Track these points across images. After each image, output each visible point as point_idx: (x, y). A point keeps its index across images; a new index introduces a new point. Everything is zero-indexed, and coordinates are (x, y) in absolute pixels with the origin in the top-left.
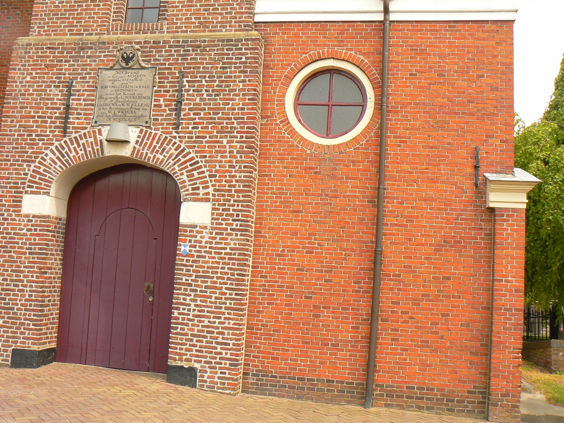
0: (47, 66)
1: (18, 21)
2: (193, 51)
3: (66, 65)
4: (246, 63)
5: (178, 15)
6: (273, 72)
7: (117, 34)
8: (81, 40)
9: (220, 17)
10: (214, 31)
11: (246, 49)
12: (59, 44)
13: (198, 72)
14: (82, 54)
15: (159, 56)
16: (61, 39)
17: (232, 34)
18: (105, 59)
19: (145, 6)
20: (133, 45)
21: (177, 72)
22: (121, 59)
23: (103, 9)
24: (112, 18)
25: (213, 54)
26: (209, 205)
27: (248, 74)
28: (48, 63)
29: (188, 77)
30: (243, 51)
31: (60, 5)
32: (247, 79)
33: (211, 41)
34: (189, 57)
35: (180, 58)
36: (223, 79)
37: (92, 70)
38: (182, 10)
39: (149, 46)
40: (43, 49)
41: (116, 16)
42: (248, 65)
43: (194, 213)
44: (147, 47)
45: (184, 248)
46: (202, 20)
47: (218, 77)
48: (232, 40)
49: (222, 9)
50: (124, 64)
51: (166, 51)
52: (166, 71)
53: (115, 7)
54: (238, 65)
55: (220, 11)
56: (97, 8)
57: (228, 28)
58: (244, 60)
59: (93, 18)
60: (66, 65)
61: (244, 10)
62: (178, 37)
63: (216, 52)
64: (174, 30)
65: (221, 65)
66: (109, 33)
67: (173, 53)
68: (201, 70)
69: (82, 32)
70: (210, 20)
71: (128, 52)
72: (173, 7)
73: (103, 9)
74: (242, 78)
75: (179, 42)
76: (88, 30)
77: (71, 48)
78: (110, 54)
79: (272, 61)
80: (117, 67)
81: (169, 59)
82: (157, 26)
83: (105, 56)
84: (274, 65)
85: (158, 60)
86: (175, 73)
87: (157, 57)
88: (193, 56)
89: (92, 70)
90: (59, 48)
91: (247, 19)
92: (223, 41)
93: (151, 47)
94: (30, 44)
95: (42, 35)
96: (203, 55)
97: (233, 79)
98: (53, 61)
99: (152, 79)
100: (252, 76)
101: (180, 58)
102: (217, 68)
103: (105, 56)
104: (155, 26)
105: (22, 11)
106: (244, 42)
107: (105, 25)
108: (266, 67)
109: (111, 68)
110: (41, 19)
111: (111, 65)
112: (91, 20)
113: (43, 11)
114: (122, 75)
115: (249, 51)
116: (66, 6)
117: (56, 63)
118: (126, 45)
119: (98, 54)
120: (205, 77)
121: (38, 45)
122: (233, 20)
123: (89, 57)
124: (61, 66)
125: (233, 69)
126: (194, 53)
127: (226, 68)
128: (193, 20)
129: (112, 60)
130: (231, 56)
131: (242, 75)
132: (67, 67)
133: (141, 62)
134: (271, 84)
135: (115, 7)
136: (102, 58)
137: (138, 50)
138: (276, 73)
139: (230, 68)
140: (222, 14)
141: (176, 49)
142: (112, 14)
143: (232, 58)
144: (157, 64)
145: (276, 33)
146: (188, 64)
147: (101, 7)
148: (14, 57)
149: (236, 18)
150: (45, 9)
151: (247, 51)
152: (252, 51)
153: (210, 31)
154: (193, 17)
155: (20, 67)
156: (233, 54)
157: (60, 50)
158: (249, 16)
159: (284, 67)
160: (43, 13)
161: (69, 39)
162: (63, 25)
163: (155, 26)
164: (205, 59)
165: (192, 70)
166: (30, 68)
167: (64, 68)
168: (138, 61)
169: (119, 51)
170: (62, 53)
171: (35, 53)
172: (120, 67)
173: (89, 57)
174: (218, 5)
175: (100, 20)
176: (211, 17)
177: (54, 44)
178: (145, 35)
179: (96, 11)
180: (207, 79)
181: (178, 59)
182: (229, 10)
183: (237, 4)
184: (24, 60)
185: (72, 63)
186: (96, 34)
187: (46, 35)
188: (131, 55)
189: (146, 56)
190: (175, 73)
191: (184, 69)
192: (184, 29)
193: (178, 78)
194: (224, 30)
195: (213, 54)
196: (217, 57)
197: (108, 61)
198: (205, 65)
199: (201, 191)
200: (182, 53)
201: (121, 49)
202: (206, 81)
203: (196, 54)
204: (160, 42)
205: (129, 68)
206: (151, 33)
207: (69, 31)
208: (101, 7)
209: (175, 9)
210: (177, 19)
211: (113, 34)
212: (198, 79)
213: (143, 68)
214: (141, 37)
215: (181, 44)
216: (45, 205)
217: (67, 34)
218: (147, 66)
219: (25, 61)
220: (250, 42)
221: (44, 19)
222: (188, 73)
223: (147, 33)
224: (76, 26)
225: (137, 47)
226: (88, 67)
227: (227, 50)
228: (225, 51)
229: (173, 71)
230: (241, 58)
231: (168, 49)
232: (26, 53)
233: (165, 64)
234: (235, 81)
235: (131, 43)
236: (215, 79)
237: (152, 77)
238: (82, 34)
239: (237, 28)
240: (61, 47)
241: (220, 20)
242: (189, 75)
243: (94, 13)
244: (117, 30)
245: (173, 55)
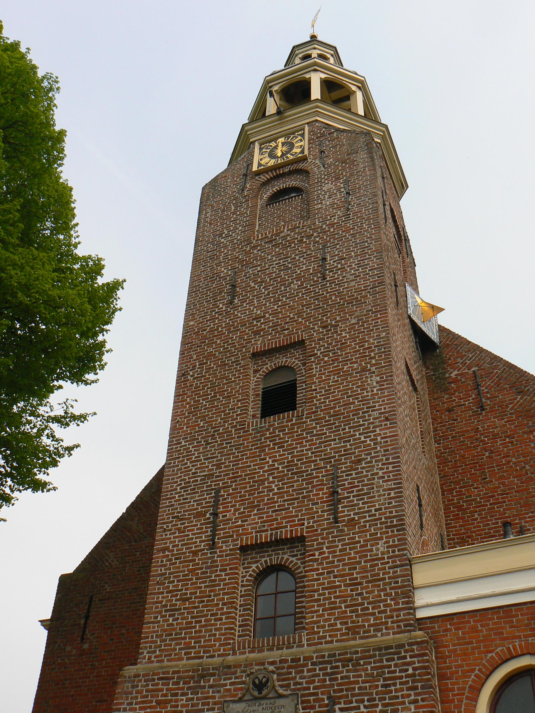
0: (158, 702)
1: (122, 642)
2: (343, 666)
3: (182, 700)
4: (413, 675)
5: (319, 622)
6: (452, 684)
7: (244, 653)
8: (200, 665)
9: (372, 619)
10: (367, 637)
11: (411, 657)
12: (174, 672)
13: (353, 695)
14: (202, 683)
15: (301, 678)
16: (176, 666)
17: (390, 638)
18: (232, 687)
19: (278, 614)
20: (267, 666)
21: (325, 697)
22: (251, 686)
23: (225, 624)
24: (237, 634)
25: (369, 668)
27: (420, 690)
28: (160, 698)
29: (340, 703)
30: (409, 659)
31: (175, 623)
32: (419, 698)
33: (365, 651)
34: (339, 676)
35: (327, 678)
36: (387, 701)
37: (215, 703)
38: (323, 615)
39: (286, 665)
40: (154, 680)
41: (242, 631)
42: (417, 678)
44: (283, 668)
46: (350, 625)
47: (380, 699)
48: (391, 647)
49: (373, 608)
50: (256, 693)
51: (308, 671)
52: (312, 698)
53: (241, 619)
54: (404, 679)
55: (371, 611)
56: (219, 623)
57: (384, 631)
58: (410, 671)
59: (215, 635)
60: (182, 700)
61: (401, 606)
62: (321, 650)
63: (373, 665)
64: (316, 641)
65: (382, 682)
66: (234, 654)
67: (317, 671)
68: (357, 691)
69: (202, 654)
70: (360, 623)
71: (260, 677)
72: (312, 612)
73: (225, 624)
74: (412, 697)
75: (323, 657)
76: (209, 651)
77: (188, 677)
78: (237, 680)
79: (449, 668)
80: (246, 698)
81: (314, 681)
82: (294, 639)
83: (231, 684)
84: (452, 674)
85: (300, 684)
86: (323, 700)
87: (298, 679)
88: (345, 674)
89: (215, 703)
90: (174, 678)
91: (407, 617)
92: (380, 649)
93: (289, 667)
94: (139, 676)
95: (153, 662)
96: (357, 671)
97: (400, 700)
98: (166, 695)
99: (294, 710)
100: (425, 693)
101: (327, 678)
102: (377, 686)
103: (231, 684)
104: (291, 639)
105: (128, 629)
106: (407, 647)
107: (229, 644)
108: (442, 677)
109: (240, 700)
110: (152, 642)
111: (240, 696)
112: (213, 638)
113: (154, 632)
114: (254, 708)
115: (416, 659)
116: (182, 623)
117: (169, 698)
118: (257, 667)
119: (222, 682)
120: (363, 701)
121: (148, 675)
122: (390, 620)
123: (211, 687)
124: (176, 701)
125: (398, 686)
126: (345, 669)
127: (389, 685)
128: (339, 626)
129: (241, 689)
130: (393, 668)
131: (412, 693)
132: (184, 702)
133: (278, 688)
134: (453, 701)
135: (241, 619)
136: (228, 687)
137: (273, 672)
138: (456, 684)
139: (395, 684)
140: (373, 614)
141: (321, 666)
142: (237, 628)
143: (395, 672)
144: (299, 689)
145: (447, 630)
146: (338, 685)
147: (224, 621)
148: (119, 693)
149: (393, 617)
150: (156, 629)
151: (413, 659)
152: (420, 659)
153: (362, 638)
154: (338, 622)
155: (125, 706)
156: (396, 665)
157: (175, 680)
158: (408, 613)
159: (466, 674)
160: (155, 635)
161: (185, 665)
162: (178, 647)
163: (291, 639)
164: (361, 676)
165: (345, 693)
166: (138, 706)
167: (180, 703)
168: (274, 687)
169: (248, 675)
170: (178, 683)
171: (145, 686)
172: (251, 698)
173: (211, 687)
174: (368, 604)
175: (223, 638)
176: (360, 619)
177: (168, 673)
178: (280, 652)
179: (218, 626)
180: (366, 703)
181: (325, 680)
182: (382, 608)
183: (391, 600)
184: (130, 696)
185: (190, 696)
186: (219, 656)
187: (158, 661)
188: (264, 680)
189: (284, 680)
190: (323, 700)
191: (334, 692)
192: (328, 639)
193: (327, 705)
194: (379, 634)
195: (369, 668)
196: (375, 672)
197: (235, 689)
198: (361, 685)
200: (329, 671)
201: (251, 673)
202: (365, 707)
203: (348, 671)
204: (300, 659)
205: (265, 698)
206: (287, 648)
207: (185, 654)
208: (224, 621)
209: (315, 615)
210: (318, 627)
211: (241, 653)
212: (354, 704)
213: (281, 696)
214: (275, 655)
215: (326, 659)
217: (183, 659)
218: (285, 693)
219: (132, 698)
220: (415, 647)
221: (156, 642)
222: (340, 697)
223: (282, 649)
224: (194, 647)
225: (271, 668)
226: (211, 701)
227: (387, 660)
228: (385, 663)
229: (320, 696)
230: (407, 670)
231: (310, 667)
232: (133, 687)
233: (309, 689)
234: (403, 703)
235: (263, 664)
236: (377, 702)
237: (294, 708)
238: (202, 657)
239: (396, 630)
240: (176, 676)
241: (372, 622)
242: (342, 701)
243: (216, 630)
244: (244, 648)
245: (319, 675)
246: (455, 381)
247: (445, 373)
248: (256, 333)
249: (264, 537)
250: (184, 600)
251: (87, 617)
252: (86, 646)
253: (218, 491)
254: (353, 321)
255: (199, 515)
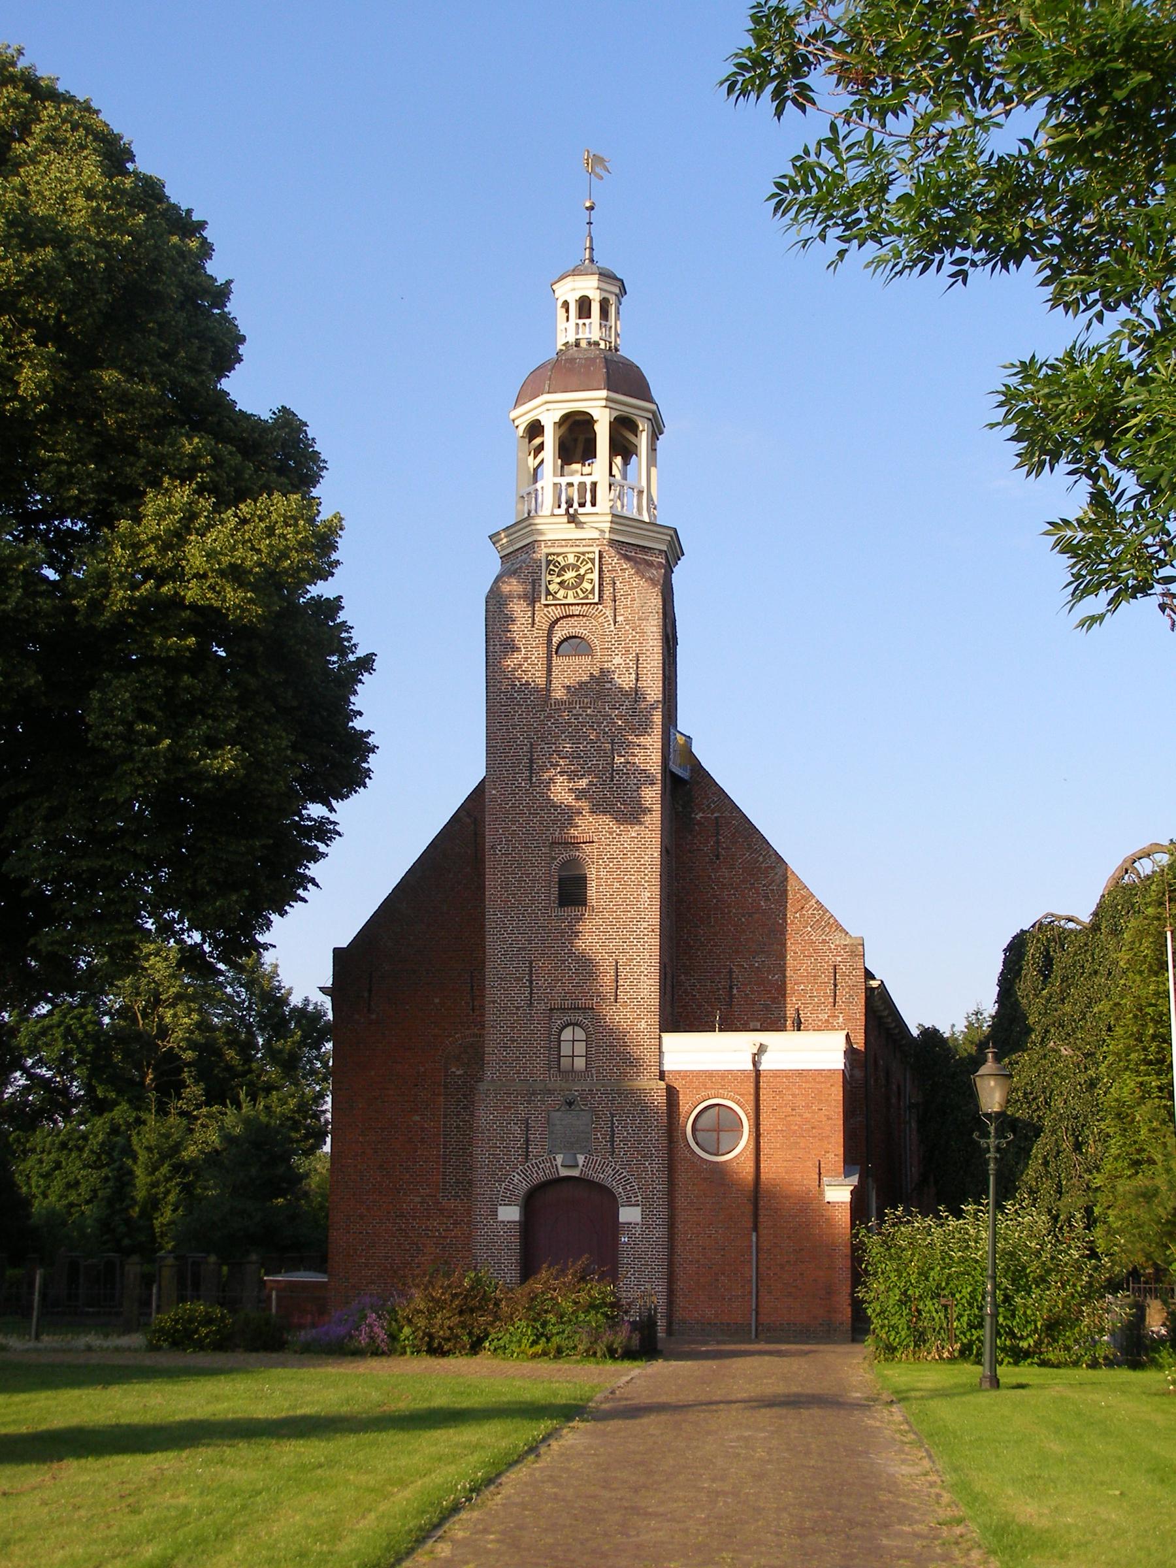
26: (639, 1209)
43: (629, 1215)
45: (624, 1239)
199: (633, 1199)
216: (510, 1213)
246: (699, 823)
247: (691, 813)
248: (554, 822)
249: (568, 1004)
250: (513, 1041)
251: (370, 991)
252: (374, 1017)
253: (531, 963)
254: (634, 835)
255: (519, 979)
